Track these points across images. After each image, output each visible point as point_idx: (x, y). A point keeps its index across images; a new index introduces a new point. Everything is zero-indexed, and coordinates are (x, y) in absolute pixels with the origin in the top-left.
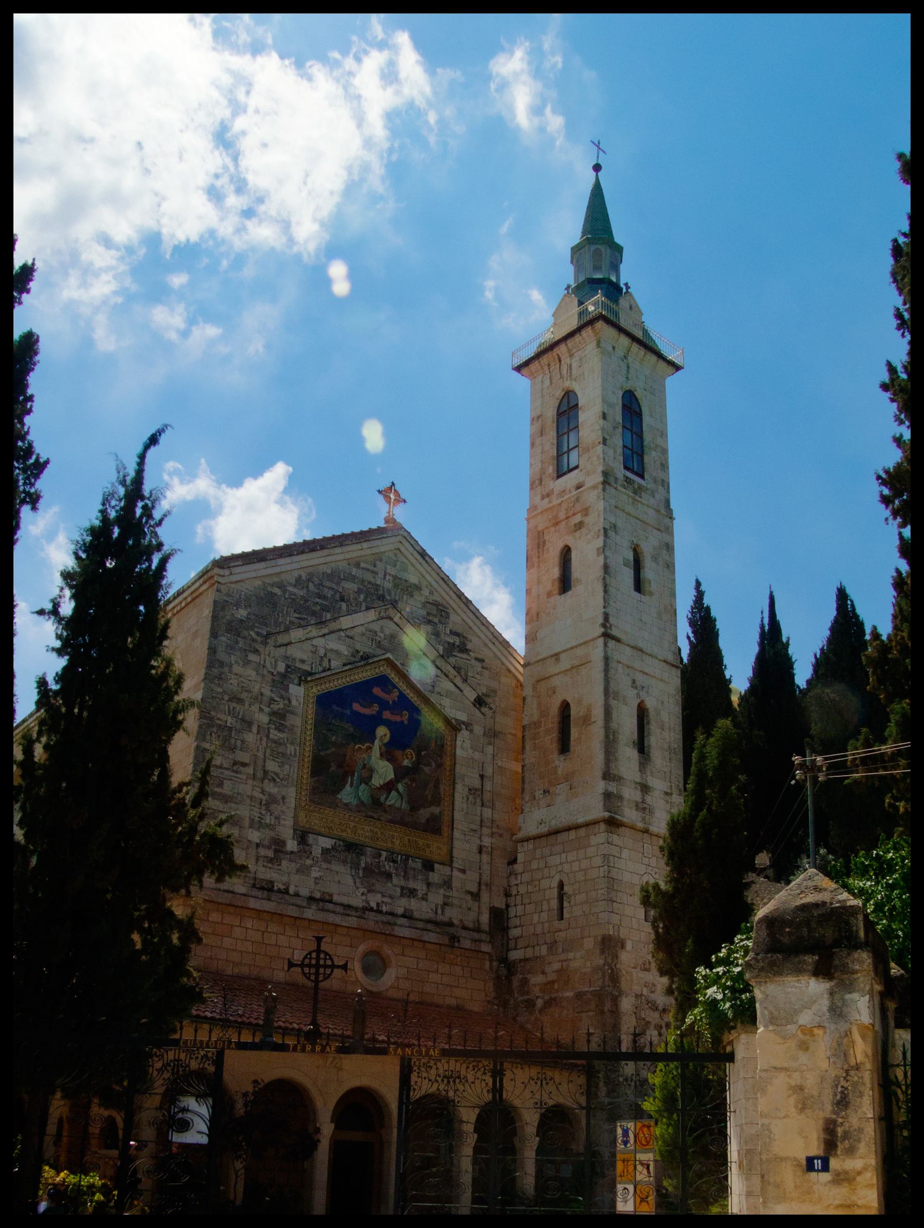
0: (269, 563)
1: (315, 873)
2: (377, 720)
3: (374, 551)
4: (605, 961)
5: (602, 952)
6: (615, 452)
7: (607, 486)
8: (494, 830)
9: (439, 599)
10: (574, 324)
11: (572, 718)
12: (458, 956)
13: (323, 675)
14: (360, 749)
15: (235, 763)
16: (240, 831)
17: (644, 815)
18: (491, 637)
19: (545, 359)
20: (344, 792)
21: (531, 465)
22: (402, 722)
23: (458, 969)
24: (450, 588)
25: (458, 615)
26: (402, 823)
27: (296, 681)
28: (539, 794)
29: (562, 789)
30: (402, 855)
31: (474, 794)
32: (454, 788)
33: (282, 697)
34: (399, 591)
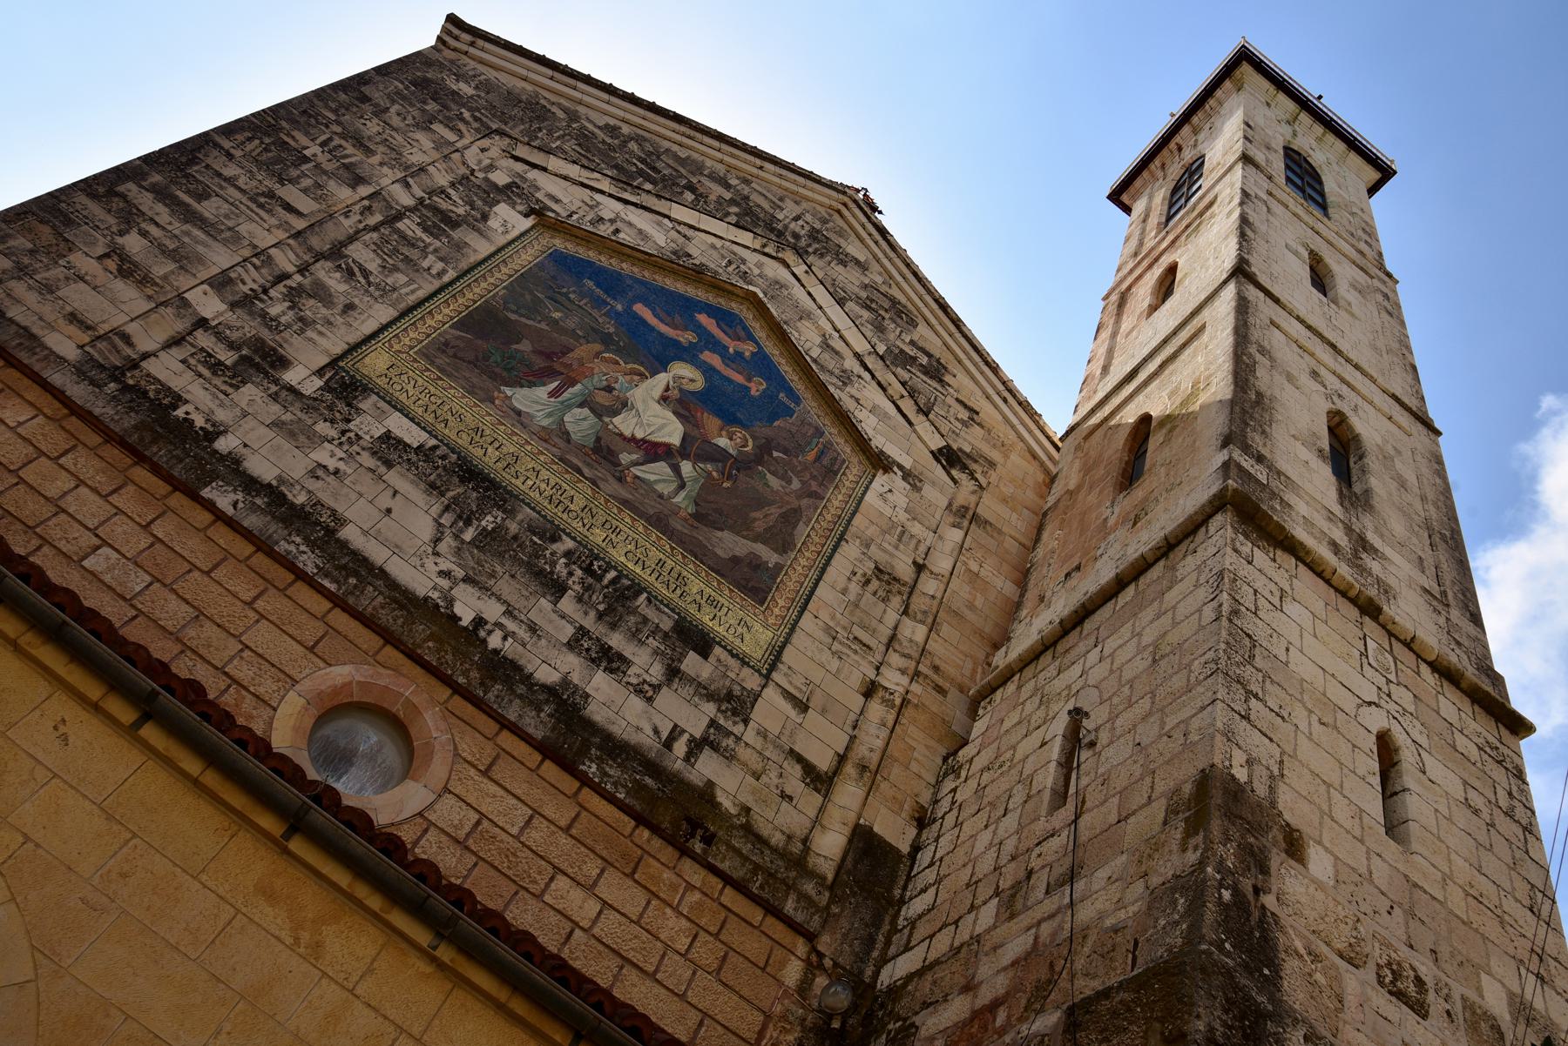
1: (322, 455)
3: (787, 184)
5: (1196, 824)
8: (921, 668)
12: (690, 887)
15: (271, 195)
16: (172, 272)
18: (1001, 387)
20: (525, 391)
22: (748, 389)
23: (673, 927)
26: (659, 522)
31: (889, 584)
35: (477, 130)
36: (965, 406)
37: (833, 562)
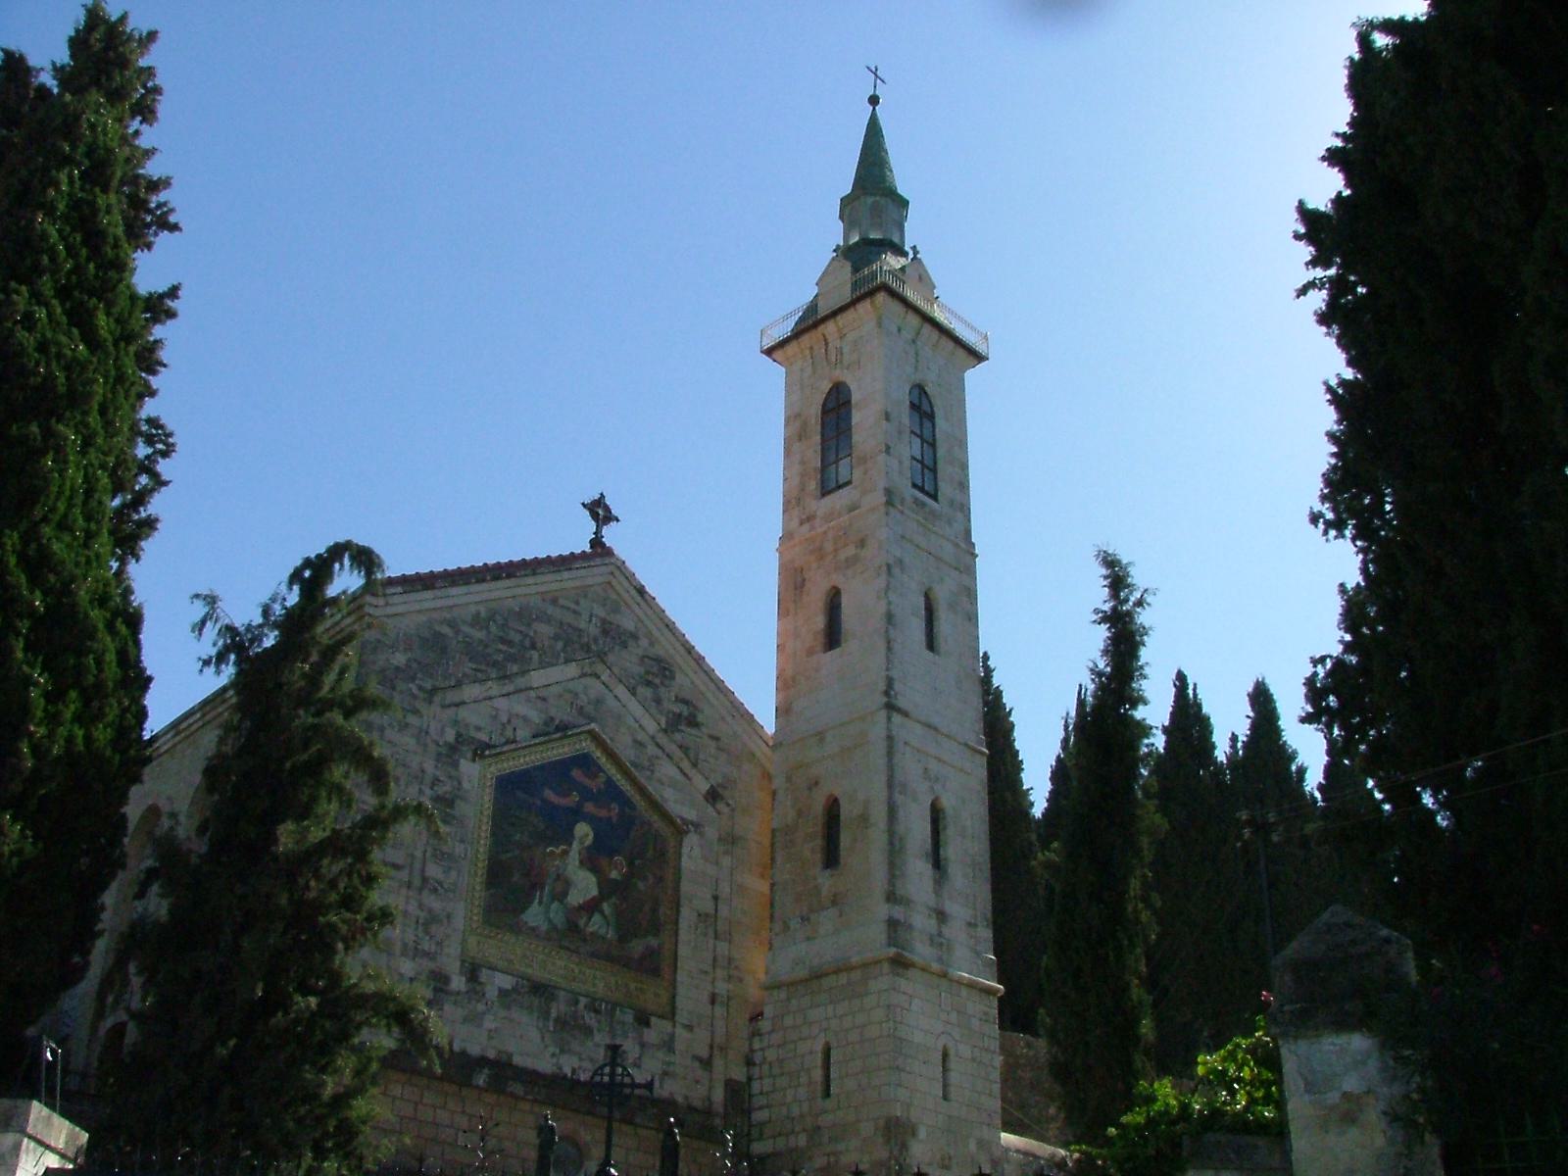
0: (438, 593)
1: (489, 1023)
2: (576, 814)
3: (578, 583)
4: (891, 1152)
5: (888, 1142)
6: (900, 462)
7: (891, 510)
9: (661, 653)
10: (846, 294)
11: (842, 818)
13: (505, 749)
14: (552, 852)
17: (940, 953)
19: (806, 339)
21: (785, 480)
22: (610, 818)
24: (678, 640)
25: (687, 675)
26: (610, 958)
27: (469, 755)
28: (794, 924)
29: (827, 920)
30: (607, 1003)
32: (678, 912)
33: (450, 777)
34: (608, 640)
35: (425, 699)
36: (712, 738)
37: (681, 926)
